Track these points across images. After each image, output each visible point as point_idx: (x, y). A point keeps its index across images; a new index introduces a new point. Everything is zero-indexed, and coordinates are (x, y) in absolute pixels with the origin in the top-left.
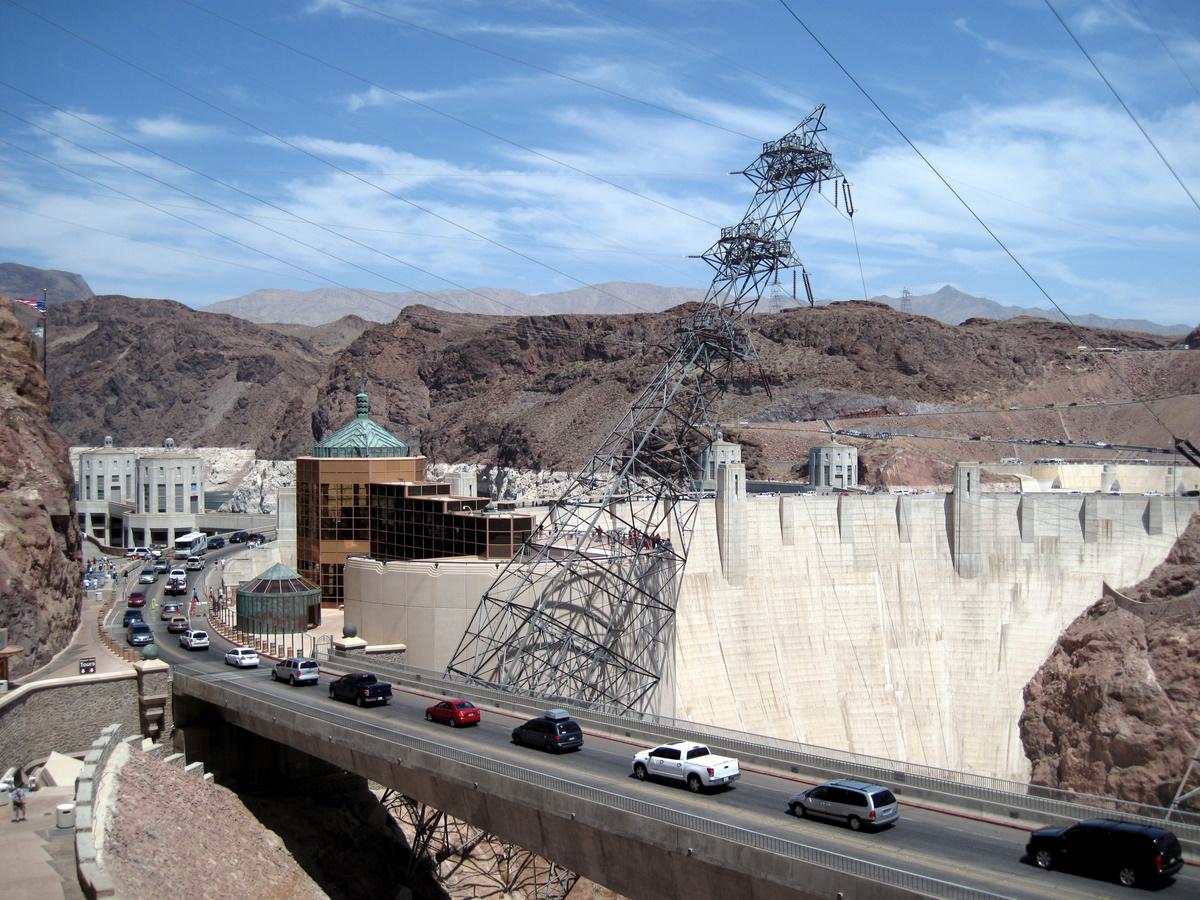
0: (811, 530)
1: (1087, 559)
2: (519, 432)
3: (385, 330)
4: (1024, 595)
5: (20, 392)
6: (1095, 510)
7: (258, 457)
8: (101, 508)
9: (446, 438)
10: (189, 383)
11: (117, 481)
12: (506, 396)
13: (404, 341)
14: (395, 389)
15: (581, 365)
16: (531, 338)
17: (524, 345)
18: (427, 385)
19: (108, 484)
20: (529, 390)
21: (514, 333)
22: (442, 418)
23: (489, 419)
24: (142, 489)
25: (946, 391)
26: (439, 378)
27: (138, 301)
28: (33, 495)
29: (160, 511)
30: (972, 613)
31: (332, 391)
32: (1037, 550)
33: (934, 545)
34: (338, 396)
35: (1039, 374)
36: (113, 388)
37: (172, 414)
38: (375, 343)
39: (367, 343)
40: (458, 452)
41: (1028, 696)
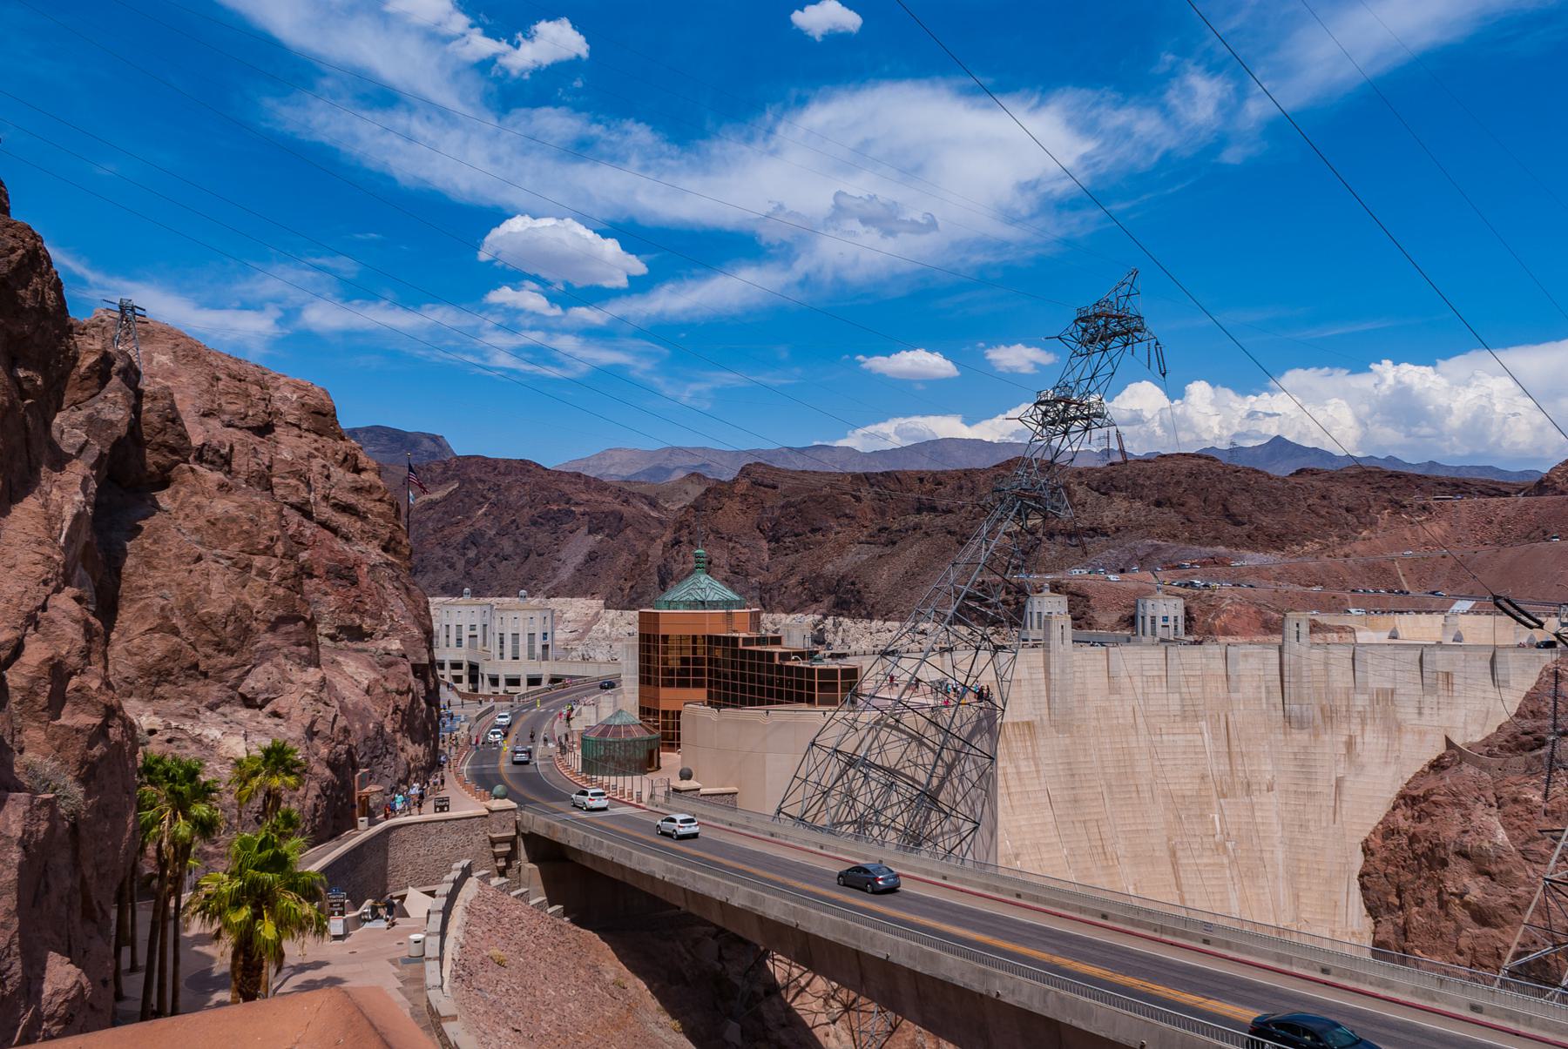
0: (1138, 681)
1: (1426, 711)
2: (853, 584)
4: (1359, 747)
5: (385, 549)
6: (1434, 662)
7: (607, 607)
8: (462, 655)
10: (543, 537)
12: (841, 549)
15: (913, 519)
22: (780, 570)
23: (824, 571)
25: (1276, 541)
27: (496, 460)
28: (395, 645)
30: (1305, 766)
32: (1371, 701)
33: (1264, 695)
35: (1373, 523)
36: (474, 540)
37: (526, 567)
40: (794, 602)
41: (1367, 850)
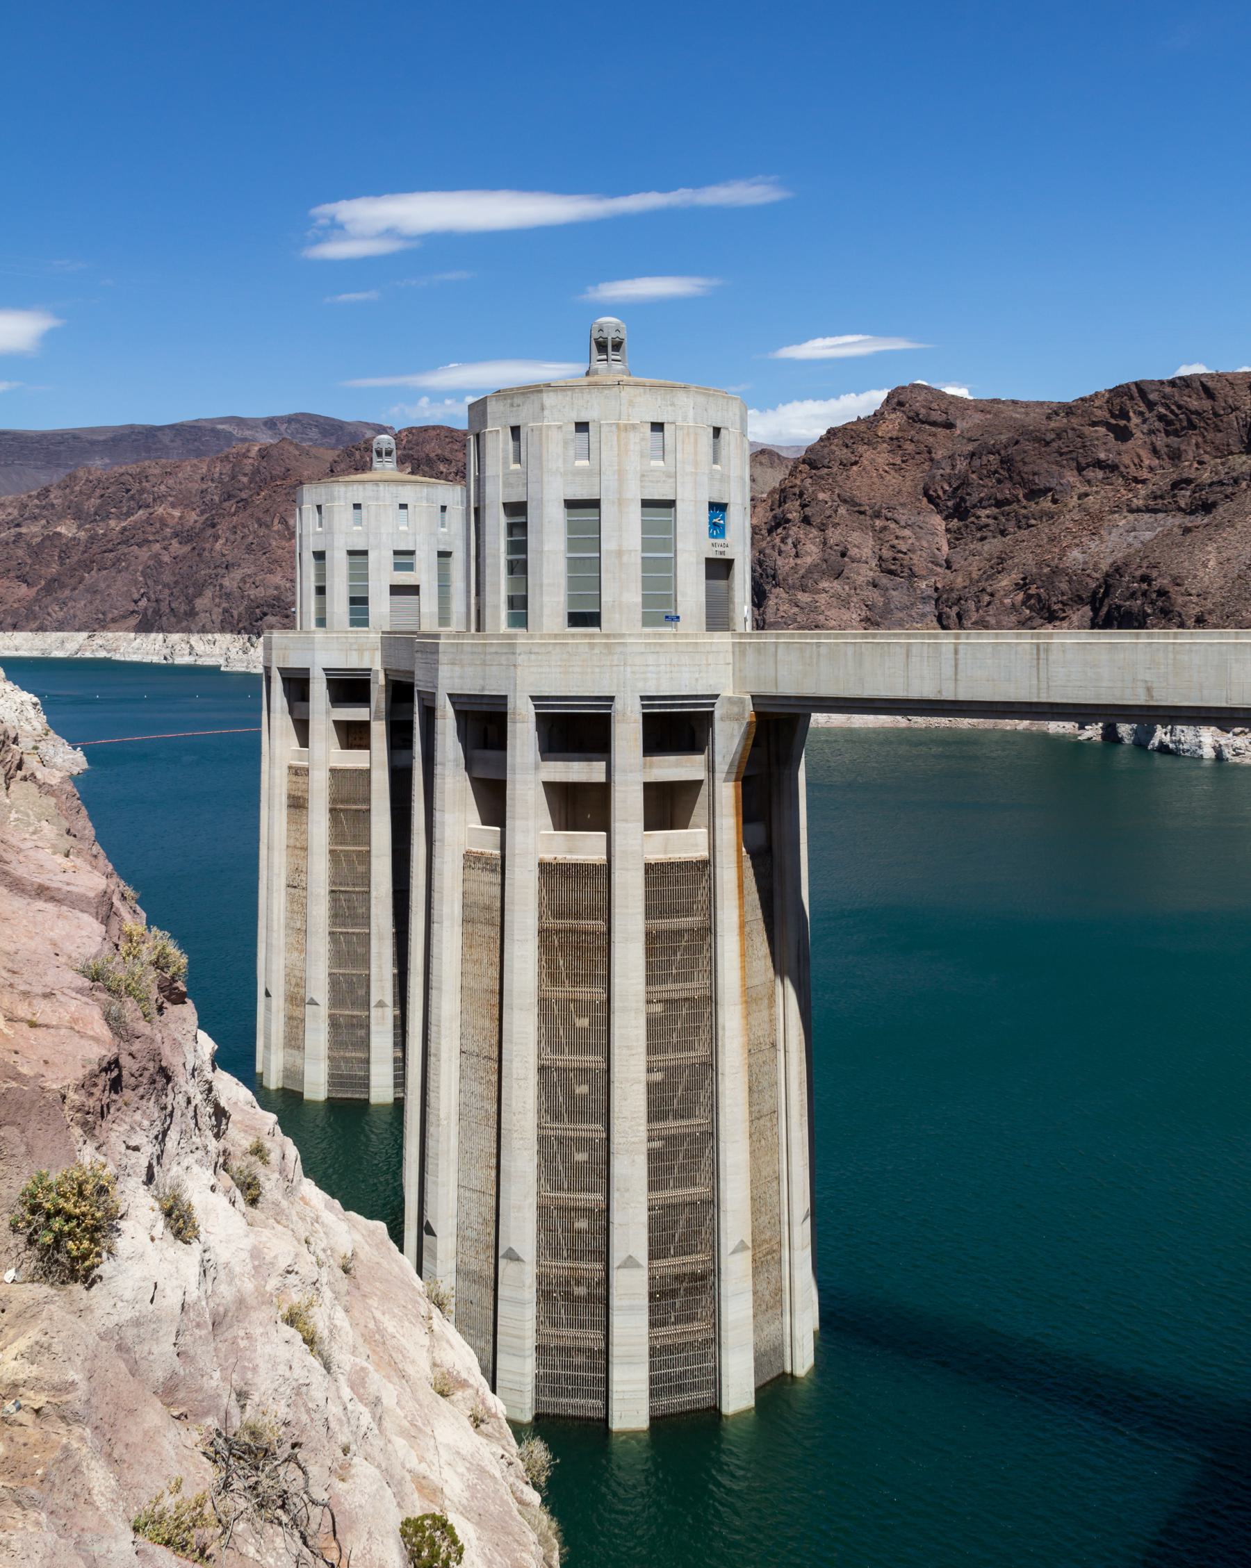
2: (1145, 579)
3: (863, 427)
8: (363, 653)
9: (987, 598)
11: (410, 567)
12: (1094, 522)
13: (896, 443)
14: (887, 519)
16: (1135, 420)
17: (1123, 434)
18: (940, 512)
19: (381, 576)
20: (1138, 510)
21: (1102, 414)
22: (975, 566)
24: (497, 523)
26: (963, 500)
29: (577, 619)
31: (778, 526)
34: (791, 532)
38: (847, 446)
39: (833, 447)
